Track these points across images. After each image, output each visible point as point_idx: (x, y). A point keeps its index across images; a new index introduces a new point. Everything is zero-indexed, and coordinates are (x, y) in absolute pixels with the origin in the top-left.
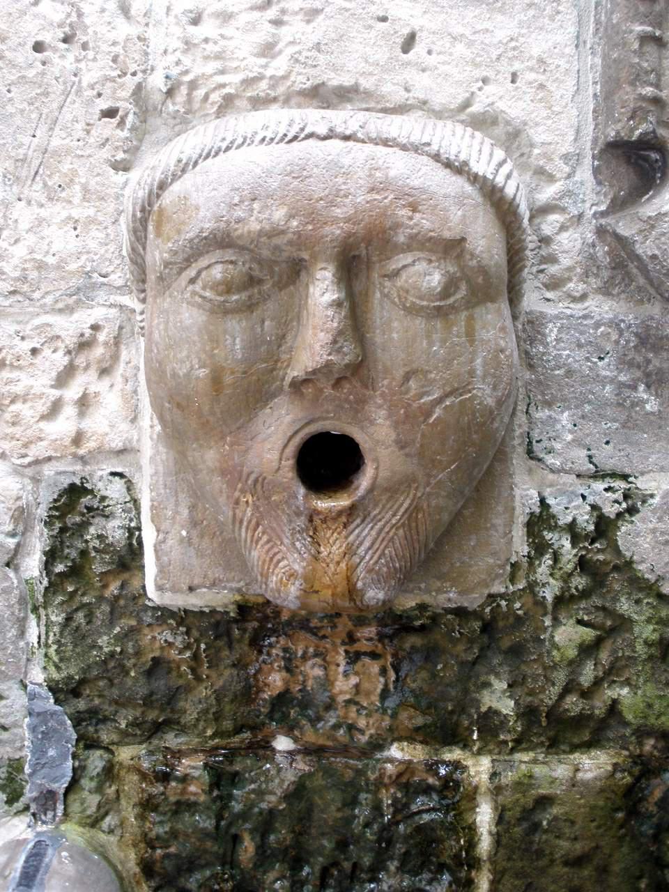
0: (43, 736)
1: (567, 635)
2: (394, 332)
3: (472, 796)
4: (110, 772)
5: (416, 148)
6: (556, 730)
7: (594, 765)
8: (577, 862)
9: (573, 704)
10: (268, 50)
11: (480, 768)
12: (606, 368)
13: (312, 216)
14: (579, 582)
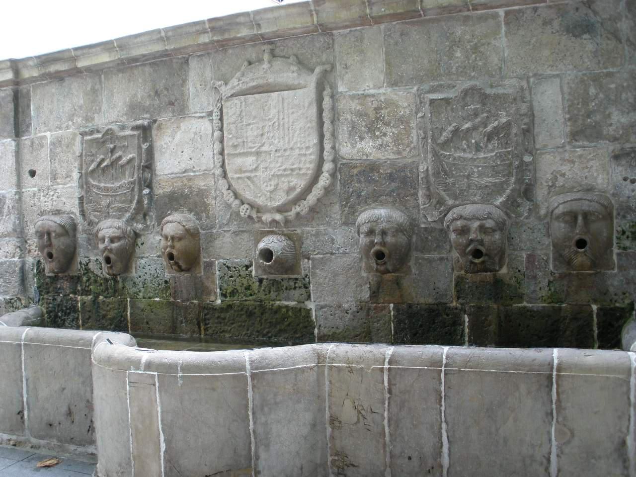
0: (36, 293)
1: (85, 279)
2: (54, 241)
3: (78, 301)
4: (43, 299)
5: (52, 221)
6: (86, 292)
7: (90, 297)
8: (90, 311)
9: (86, 289)
10: (52, 205)
11: (79, 298)
12: (85, 243)
13: (43, 228)
14: (85, 271)
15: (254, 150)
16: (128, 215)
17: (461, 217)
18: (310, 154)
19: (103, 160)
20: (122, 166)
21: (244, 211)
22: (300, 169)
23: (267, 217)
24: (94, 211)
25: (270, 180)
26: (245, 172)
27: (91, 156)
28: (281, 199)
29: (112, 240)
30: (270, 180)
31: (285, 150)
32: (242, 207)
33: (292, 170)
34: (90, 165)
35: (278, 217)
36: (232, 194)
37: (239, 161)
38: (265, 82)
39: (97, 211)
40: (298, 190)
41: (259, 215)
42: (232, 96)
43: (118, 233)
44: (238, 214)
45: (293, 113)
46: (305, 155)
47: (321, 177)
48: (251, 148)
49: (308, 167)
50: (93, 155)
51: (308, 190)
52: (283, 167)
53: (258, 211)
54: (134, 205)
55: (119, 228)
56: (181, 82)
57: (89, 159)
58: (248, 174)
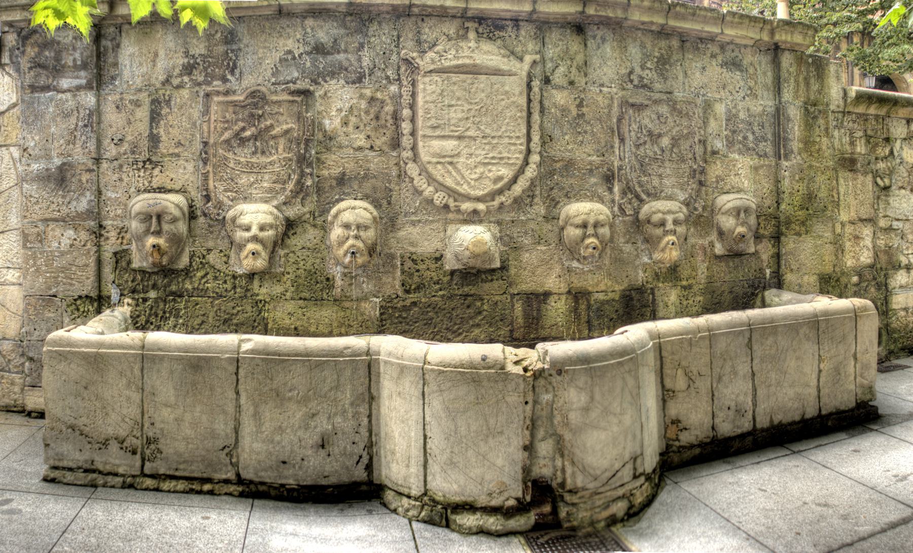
15: (457, 134)
16: (282, 198)
17: (659, 211)
18: (521, 144)
19: (243, 129)
20: (274, 137)
21: (439, 198)
22: (509, 158)
23: (467, 206)
24: (225, 191)
25: (475, 167)
26: (444, 157)
27: (224, 122)
28: (488, 187)
29: (262, 228)
30: (475, 167)
31: (493, 137)
32: (437, 195)
33: (501, 159)
34: (222, 134)
35: (481, 207)
36: (425, 180)
37: (436, 144)
38: (472, 62)
39: (231, 191)
40: (506, 180)
41: (457, 204)
42: (431, 71)
43: (269, 219)
44: (430, 202)
45: (503, 100)
46: (515, 144)
47: (528, 168)
48: (452, 131)
49: (517, 158)
50: (227, 122)
51: (514, 180)
52: (491, 155)
53: (455, 200)
54: (291, 186)
55: (271, 213)
56: (356, 45)
57: (220, 125)
58: (448, 159)
